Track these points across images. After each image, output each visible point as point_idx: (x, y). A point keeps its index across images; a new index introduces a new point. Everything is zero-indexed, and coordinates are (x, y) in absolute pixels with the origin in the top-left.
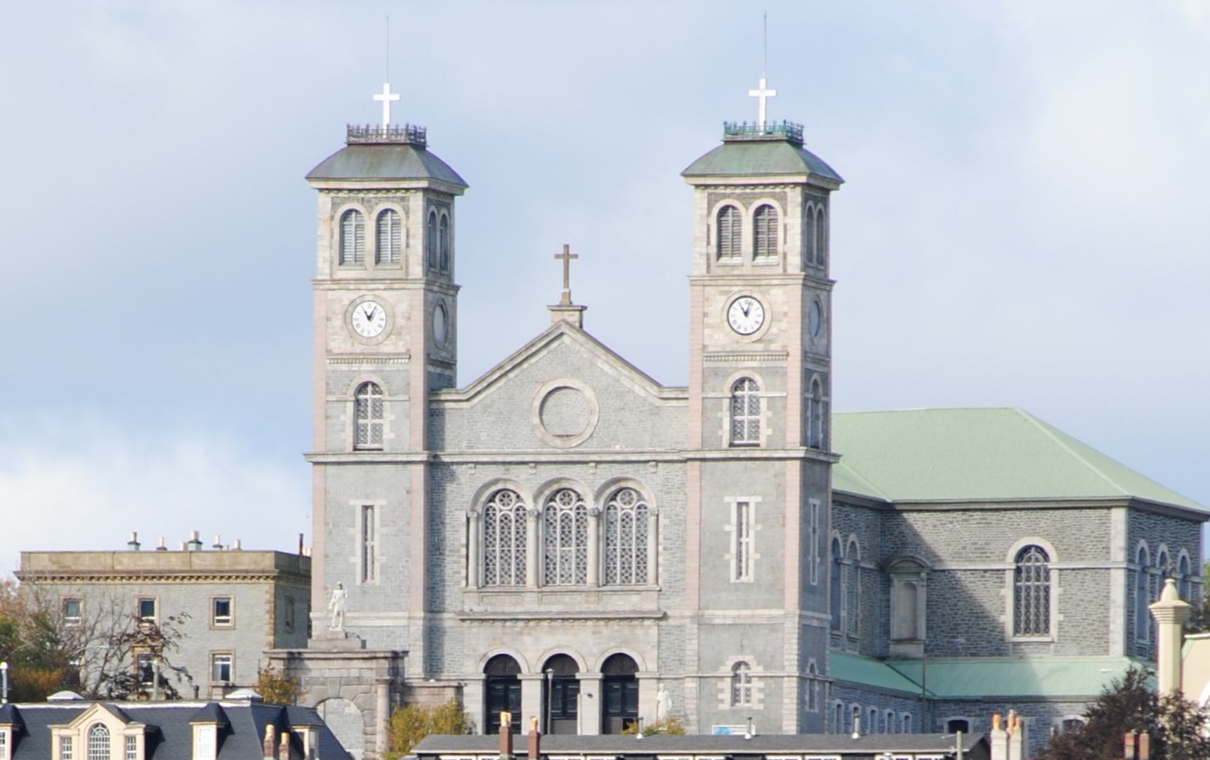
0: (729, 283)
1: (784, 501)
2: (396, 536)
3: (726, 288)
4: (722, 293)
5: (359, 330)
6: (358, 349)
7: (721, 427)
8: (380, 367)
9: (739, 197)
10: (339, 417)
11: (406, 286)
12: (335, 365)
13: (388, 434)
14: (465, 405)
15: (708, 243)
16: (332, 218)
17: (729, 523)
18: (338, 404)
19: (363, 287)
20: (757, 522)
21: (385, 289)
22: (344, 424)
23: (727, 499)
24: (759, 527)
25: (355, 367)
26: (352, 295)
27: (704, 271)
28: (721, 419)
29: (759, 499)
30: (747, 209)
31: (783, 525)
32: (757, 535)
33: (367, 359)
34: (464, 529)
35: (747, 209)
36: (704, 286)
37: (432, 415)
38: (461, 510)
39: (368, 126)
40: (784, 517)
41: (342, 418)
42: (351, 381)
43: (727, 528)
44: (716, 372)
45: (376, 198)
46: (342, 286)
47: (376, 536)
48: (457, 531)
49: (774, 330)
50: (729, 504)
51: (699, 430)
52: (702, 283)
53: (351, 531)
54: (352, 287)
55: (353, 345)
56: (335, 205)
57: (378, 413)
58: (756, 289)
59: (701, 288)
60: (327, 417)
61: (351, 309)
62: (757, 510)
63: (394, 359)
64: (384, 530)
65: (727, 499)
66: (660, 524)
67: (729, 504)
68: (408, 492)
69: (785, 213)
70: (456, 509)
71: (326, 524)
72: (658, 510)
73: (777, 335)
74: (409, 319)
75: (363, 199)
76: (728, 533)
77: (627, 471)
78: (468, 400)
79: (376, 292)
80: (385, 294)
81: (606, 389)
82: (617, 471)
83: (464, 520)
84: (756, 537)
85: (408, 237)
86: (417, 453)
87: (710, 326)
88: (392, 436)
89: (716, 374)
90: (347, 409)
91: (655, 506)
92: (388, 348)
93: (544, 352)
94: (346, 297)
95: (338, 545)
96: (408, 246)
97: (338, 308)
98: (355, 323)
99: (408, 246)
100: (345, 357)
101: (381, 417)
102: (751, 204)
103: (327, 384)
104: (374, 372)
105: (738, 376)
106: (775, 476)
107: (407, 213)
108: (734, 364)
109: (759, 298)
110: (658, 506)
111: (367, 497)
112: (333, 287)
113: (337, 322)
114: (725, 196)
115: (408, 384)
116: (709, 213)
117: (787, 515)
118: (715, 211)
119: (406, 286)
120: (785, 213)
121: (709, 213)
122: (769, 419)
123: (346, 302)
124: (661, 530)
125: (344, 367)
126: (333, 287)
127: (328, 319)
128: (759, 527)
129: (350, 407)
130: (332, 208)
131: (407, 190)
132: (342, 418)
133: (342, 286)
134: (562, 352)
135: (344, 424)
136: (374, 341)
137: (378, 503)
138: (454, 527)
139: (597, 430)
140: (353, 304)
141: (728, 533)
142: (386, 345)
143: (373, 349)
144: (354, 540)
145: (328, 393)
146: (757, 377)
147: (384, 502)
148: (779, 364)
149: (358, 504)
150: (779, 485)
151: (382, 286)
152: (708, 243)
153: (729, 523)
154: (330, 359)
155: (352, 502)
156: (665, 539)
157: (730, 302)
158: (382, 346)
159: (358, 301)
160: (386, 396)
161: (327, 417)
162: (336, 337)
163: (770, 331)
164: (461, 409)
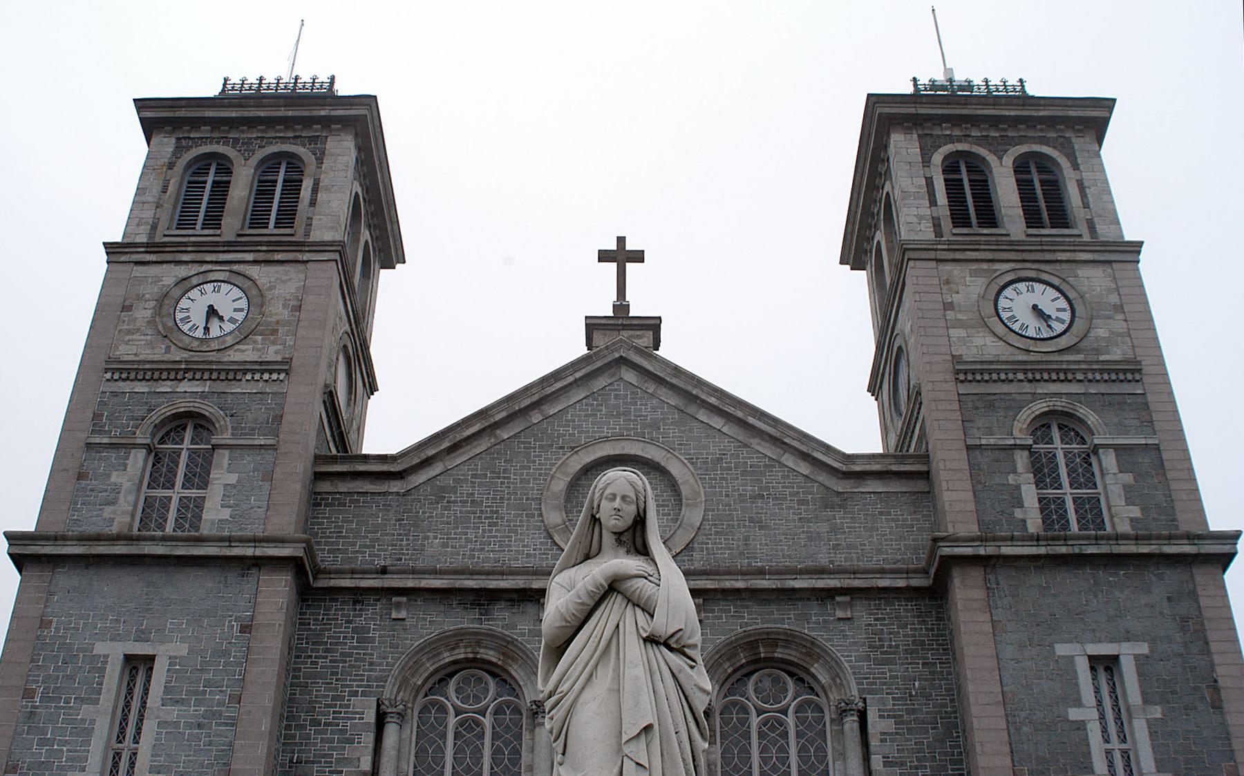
0: (990, 256)
1: (1206, 651)
2: (200, 726)
3: (985, 266)
4: (974, 274)
5: (185, 328)
6: (177, 355)
7: (1020, 504)
8: (220, 387)
9: (982, 141)
10: (109, 476)
11: (300, 257)
12: (121, 384)
13: (215, 513)
14: (396, 486)
15: (933, 202)
16: (171, 166)
17: (1078, 703)
18: (113, 455)
19: (209, 257)
20: (1146, 700)
21: (255, 262)
22: (117, 489)
23: (1062, 649)
24: (1157, 712)
25: (165, 387)
26: (183, 271)
27: (932, 236)
28: (1018, 487)
29: (1144, 649)
30: (1000, 158)
31: (1217, 706)
32: (1154, 728)
33: (195, 371)
34: (369, 739)
35: (1000, 158)
36: (938, 260)
37: (317, 505)
38: (364, 694)
39: (261, 79)
40: (1215, 687)
41: (115, 477)
42: (150, 411)
43: (1074, 714)
44: (990, 403)
45: (262, 138)
46: (168, 257)
47: (149, 726)
48: (352, 741)
49: (1101, 332)
50: (1070, 659)
51: (971, 506)
52: (932, 255)
53: (86, 711)
54: (185, 257)
55: (168, 350)
56: (179, 149)
57: (199, 476)
58: (1043, 267)
59: (933, 264)
60: (81, 476)
61: (177, 292)
62: (1141, 674)
63: (254, 372)
64: (172, 713)
65: (1062, 649)
66: (871, 730)
67: (1070, 659)
68: (246, 629)
69: (1076, 167)
70: (355, 694)
71: (28, 694)
72: (865, 699)
73: (1108, 340)
74: (299, 308)
75: (236, 141)
76: (1081, 726)
77: (784, 620)
78: (400, 475)
79: (236, 267)
80: (253, 271)
81: (720, 460)
82: (754, 620)
83: (370, 717)
84: (1152, 734)
85: (315, 190)
86: (280, 541)
87: (959, 324)
88: (226, 514)
89: (991, 406)
90: (130, 462)
91: (855, 692)
92: (247, 353)
93: (579, 394)
94: (170, 275)
95: (42, 742)
96: (313, 203)
97: (151, 290)
98: (179, 316)
99: (313, 203)
100: (147, 366)
101: (204, 484)
102: (1006, 151)
103: (97, 416)
104: (203, 395)
105: (1040, 407)
106: (1169, 599)
107: (320, 161)
108: (1027, 388)
109: (1056, 281)
110: (861, 691)
111: (142, 637)
112: (148, 257)
113: (143, 313)
114: (950, 139)
115: (279, 418)
116: (926, 162)
117: (1221, 682)
118: (937, 158)
119: (300, 257)
120: (1076, 167)
121: (926, 162)
122: (1126, 487)
123: (169, 281)
124: (874, 742)
125: (141, 387)
126: (148, 257)
127: (126, 308)
128: (1157, 712)
129: (137, 459)
130: (174, 153)
131: (327, 122)
132: (115, 477)
133: (168, 257)
134: (616, 397)
135: (117, 489)
136: (215, 346)
137: (166, 652)
138: (344, 732)
139: (700, 538)
140: (185, 285)
141: (1081, 726)
142: (238, 350)
143: (212, 357)
144: (86, 733)
145: (97, 429)
146: (1083, 411)
147: (182, 650)
148: (1126, 388)
149: (114, 651)
150: (1185, 620)
151: (250, 257)
152: (933, 202)
153: (1078, 703)
154: (114, 371)
155: (100, 648)
156: (886, 764)
157: (995, 288)
158: (231, 352)
159: (195, 281)
160: (226, 437)
161: (81, 476)
162: (135, 337)
163: (1092, 334)
164: (385, 494)
